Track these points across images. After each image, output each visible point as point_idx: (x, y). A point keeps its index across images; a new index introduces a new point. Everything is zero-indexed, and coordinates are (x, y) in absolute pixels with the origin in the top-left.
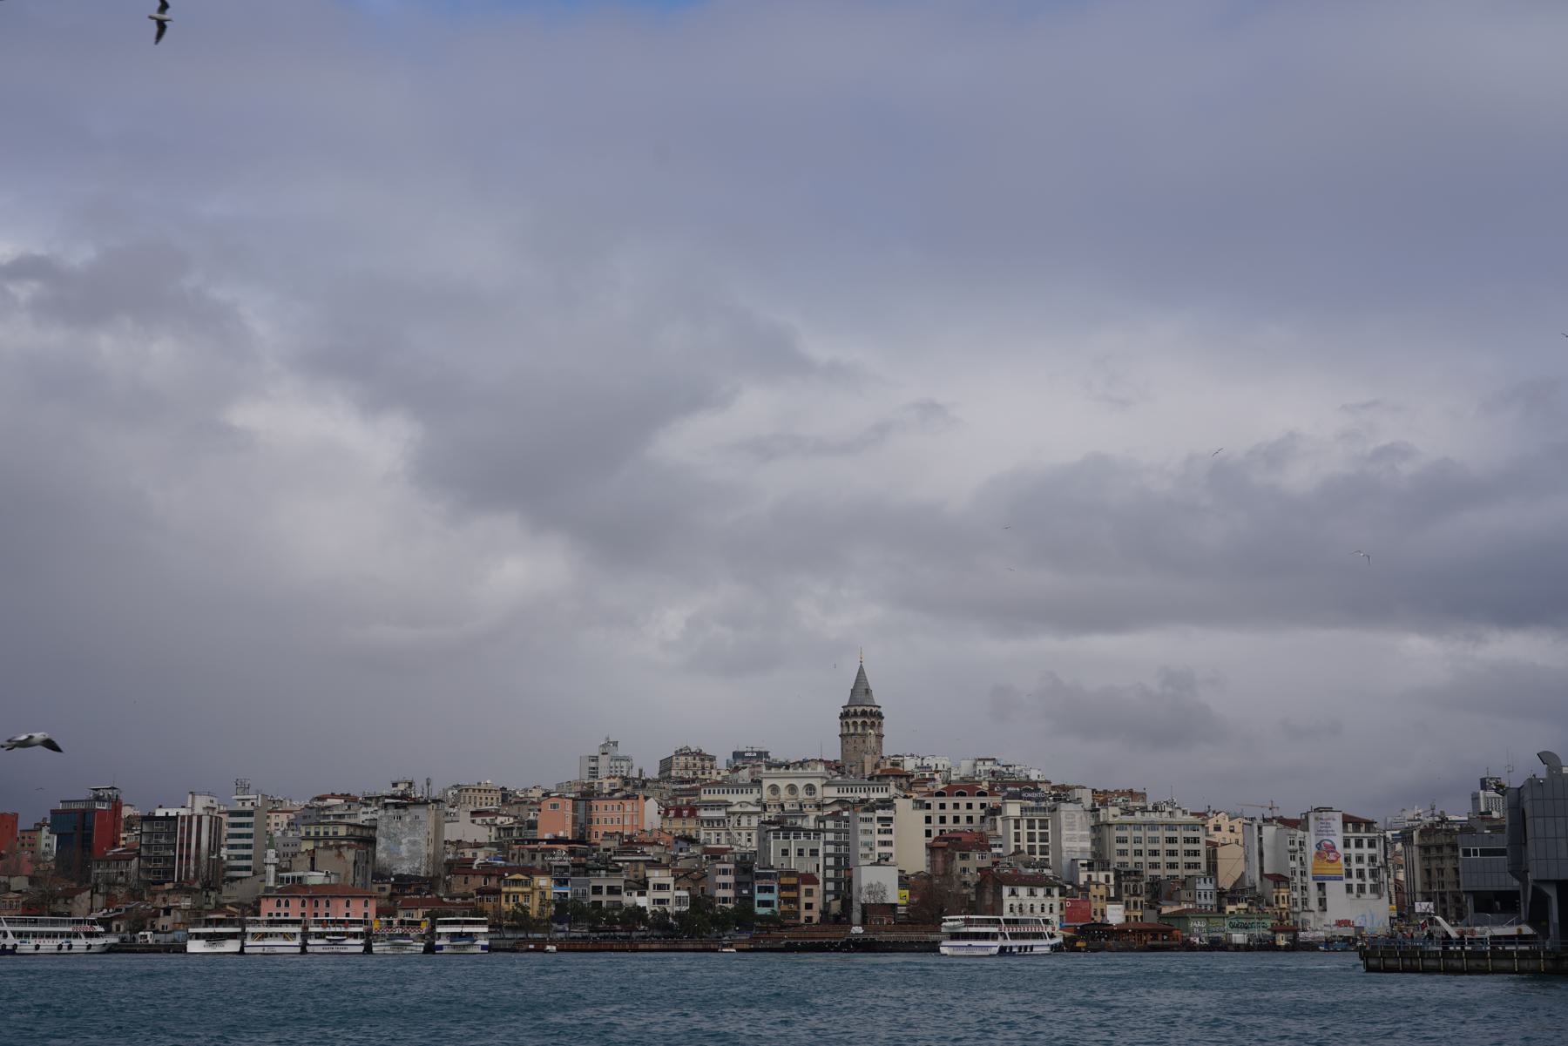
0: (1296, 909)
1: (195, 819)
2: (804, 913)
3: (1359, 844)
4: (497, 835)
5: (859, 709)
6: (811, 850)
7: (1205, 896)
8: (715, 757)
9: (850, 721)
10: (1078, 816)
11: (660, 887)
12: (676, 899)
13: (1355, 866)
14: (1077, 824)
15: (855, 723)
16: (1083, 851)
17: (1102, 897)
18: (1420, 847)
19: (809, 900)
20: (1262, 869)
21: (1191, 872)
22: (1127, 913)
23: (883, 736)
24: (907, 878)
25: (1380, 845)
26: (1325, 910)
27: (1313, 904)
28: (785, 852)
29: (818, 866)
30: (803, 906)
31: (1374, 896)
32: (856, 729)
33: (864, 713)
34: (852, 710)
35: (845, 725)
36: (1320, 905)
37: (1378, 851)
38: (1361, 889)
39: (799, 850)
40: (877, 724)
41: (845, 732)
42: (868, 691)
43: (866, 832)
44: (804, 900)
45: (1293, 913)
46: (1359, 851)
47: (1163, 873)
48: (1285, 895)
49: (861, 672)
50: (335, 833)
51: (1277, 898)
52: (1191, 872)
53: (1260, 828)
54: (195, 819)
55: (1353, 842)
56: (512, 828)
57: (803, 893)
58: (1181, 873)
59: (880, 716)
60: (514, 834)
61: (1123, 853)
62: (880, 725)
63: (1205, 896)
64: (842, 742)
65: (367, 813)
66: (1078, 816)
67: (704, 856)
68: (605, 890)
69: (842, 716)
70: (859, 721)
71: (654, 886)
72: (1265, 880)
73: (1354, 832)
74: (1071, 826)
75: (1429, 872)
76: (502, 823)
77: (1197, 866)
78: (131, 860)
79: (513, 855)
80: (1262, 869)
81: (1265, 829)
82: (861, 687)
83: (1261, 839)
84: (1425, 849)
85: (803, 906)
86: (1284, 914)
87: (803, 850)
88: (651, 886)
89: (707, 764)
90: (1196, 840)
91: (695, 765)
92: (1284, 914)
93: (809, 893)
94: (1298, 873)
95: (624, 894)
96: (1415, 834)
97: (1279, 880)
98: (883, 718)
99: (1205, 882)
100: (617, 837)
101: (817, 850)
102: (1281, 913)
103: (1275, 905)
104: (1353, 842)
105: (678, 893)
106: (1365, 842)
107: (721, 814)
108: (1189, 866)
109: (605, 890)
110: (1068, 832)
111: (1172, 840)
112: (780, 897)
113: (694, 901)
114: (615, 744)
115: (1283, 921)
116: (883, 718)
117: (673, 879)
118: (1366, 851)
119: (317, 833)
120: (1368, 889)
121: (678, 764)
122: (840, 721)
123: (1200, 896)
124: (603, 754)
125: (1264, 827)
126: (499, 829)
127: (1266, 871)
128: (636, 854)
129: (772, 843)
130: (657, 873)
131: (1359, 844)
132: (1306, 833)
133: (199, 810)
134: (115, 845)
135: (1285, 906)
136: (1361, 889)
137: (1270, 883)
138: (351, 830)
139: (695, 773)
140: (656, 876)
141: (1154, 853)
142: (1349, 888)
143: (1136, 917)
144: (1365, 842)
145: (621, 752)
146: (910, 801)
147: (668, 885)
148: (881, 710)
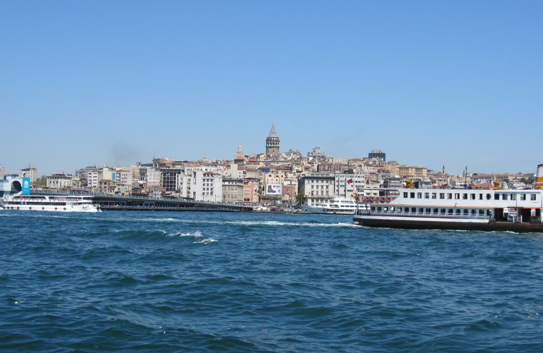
3: (208, 180)
13: (206, 187)
14: (153, 175)
32: (271, 145)
35: (267, 143)
38: (208, 193)
43: (90, 177)
46: (208, 183)
49: (273, 126)
59: (279, 141)
66: (153, 172)
69: (266, 141)
74: (151, 175)
114: (319, 148)
118: (210, 182)
120: (210, 194)
131: (208, 180)
142: (204, 194)
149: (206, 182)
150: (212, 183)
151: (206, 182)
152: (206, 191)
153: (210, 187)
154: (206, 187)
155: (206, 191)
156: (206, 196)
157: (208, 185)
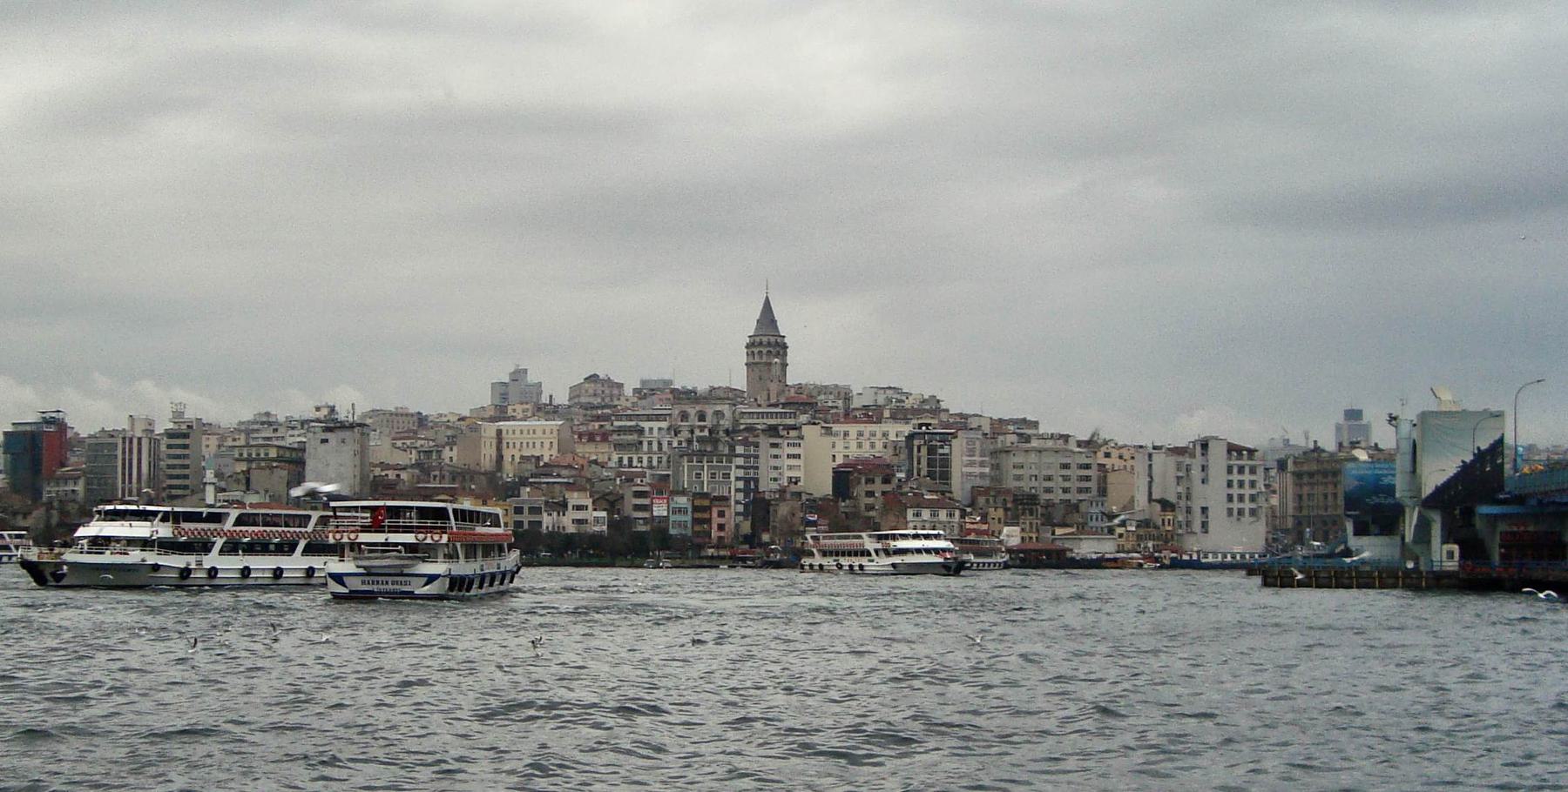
0: (1180, 531)
1: (135, 441)
2: (715, 533)
3: (1241, 470)
4: (418, 458)
5: (765, 339)
6: (723, 474)
7: (1097, 519)
8: (622, 384)
9: (756, 350)
10: (978, 443)
11: (579, 508)
12: (597, 520)
14: (977, 453)
15: (760, 352)
16: (982, 475)
17: (999, 519)
18: (1293, 473)
19: (722, 520)
20: (1150, 494)
21: (1082, 497)
22: (1025, 535)
23: (787, 365)
24: (814, 501)
25: (1260, 471)
26: (1206, 532)
27: (1197, 526)
28: (698, 475)
29: (730, 488)
30: (715, 526)
31: (1252, 519)
32: (761, 358)
33: (769, 344)
34: (758, 339)
35: (750, 354)
36: (1203, 527)
37: (1259, 477)
38: (1241, 512)
39: (712, 474)
40: (781, 353)
41: (751, 360)
42: (773, 322)
44: (716, 520)
45: (1178, 535)
46: (1241, 477)
47: (1058, 496)
48: (1171, 518)
50: (267, 454)
51: (1163, 520)
52: (1082, 497)
53: (1150, 456)
54: (135, 441)
55: (1235, 470)
56: (431, 452)
57: (715, 514)
58: (1073, 497)
59: (785, 347)
60: (434, 457)
61: (1018, 478)
62: (785, 354)
63: (1097, 519)
64: (748, 372)
65: (293, 436)
66: (978, 443)
67: (618, 479)
68: (526, 511)
69: (747, 347)
70: (765, 351)
71: (573, 506)
72: (1154, 503)
73: (1238, 459)
75: (1300, 497)
76: (422, 446)
77: (1087, 490)
78: (79, 477)
79: (435, 477)
80: (1150, 494)
81: (1155, 457)
82: (767, 317)
83: (1150, 466)
84: (1298, 475)
85: (715, 526)
86: (1169, 536)
87: (715, 474)
88: (570, 507)
89: (616, 392)
90: (1088, 467)
91: (603, 392)
92: (1169, 536)
93: (721, 514)
94: (1184, 496)
95: (545, 514)
96: (1290, 462)
97: (1166, 505)
98: (787, 347)
99: (1097, 505)
100: (533, 460)
101: (729, 474)
102: (1166, 535)
103: (1161, 527)
104: (1235, 470)
105: (596, 514)
106: (1247, 470)
107: (634, 437)
108: (1080, 490)
109: (526, 511)
110: (970, 458)
111: (1066, 466)
112: (693, 518)
113: (612, 524)
115: (1168, 542)
116: (787, 347)
117: (591, 500)
118: (1247, 477)
119: (250, 455)
121: (587, 391)
122: (746, 350)
123: (1091, 520)
124: (513, 380)
125: (1154, 455)
126: (419, 452)
127: (1155, 496)
128: (551, 475)
129: (686, 467)
130: (576, 494)
131: (1241, 470)
132: (1194, 460)
133: (139, 434)
134: (63, 465)
135: (1170, 528)
136: (1241, 512)
137: (1158, 507)
138: (281, 452)
139: (603, 399)
140: (574, 498)
141: (1049, 478)
142: (1230, 512)
143: (1031, 538)
144: (1247, 470)
145: (532, 378)
146: (819, 427)
147: (587, 507)
148: (786, 340)
149: (1236, 477)
150: (1253, 478)
151: (1236, 477)
152: (1236, 505)
153: (1247, 491)
154: (1235, 491)
155: (1236, 505)
156: (1238, 519)
157: (1241, 483)
